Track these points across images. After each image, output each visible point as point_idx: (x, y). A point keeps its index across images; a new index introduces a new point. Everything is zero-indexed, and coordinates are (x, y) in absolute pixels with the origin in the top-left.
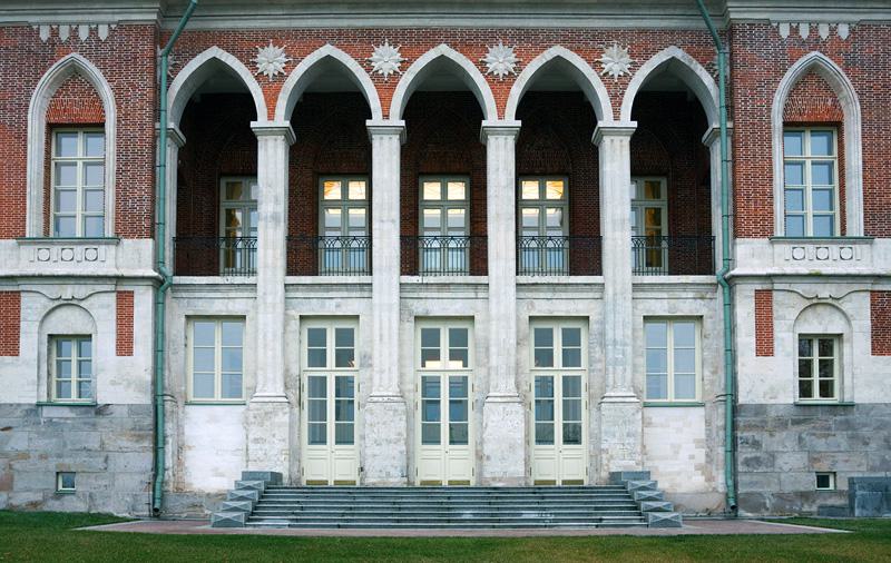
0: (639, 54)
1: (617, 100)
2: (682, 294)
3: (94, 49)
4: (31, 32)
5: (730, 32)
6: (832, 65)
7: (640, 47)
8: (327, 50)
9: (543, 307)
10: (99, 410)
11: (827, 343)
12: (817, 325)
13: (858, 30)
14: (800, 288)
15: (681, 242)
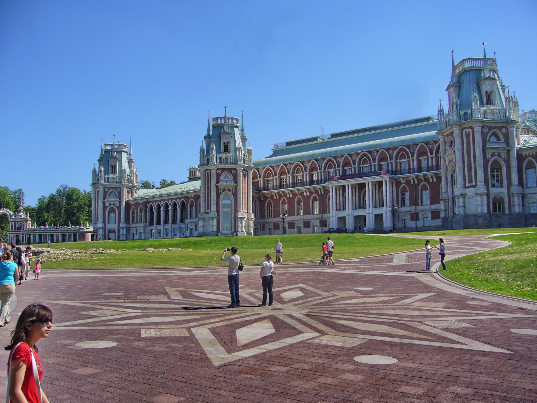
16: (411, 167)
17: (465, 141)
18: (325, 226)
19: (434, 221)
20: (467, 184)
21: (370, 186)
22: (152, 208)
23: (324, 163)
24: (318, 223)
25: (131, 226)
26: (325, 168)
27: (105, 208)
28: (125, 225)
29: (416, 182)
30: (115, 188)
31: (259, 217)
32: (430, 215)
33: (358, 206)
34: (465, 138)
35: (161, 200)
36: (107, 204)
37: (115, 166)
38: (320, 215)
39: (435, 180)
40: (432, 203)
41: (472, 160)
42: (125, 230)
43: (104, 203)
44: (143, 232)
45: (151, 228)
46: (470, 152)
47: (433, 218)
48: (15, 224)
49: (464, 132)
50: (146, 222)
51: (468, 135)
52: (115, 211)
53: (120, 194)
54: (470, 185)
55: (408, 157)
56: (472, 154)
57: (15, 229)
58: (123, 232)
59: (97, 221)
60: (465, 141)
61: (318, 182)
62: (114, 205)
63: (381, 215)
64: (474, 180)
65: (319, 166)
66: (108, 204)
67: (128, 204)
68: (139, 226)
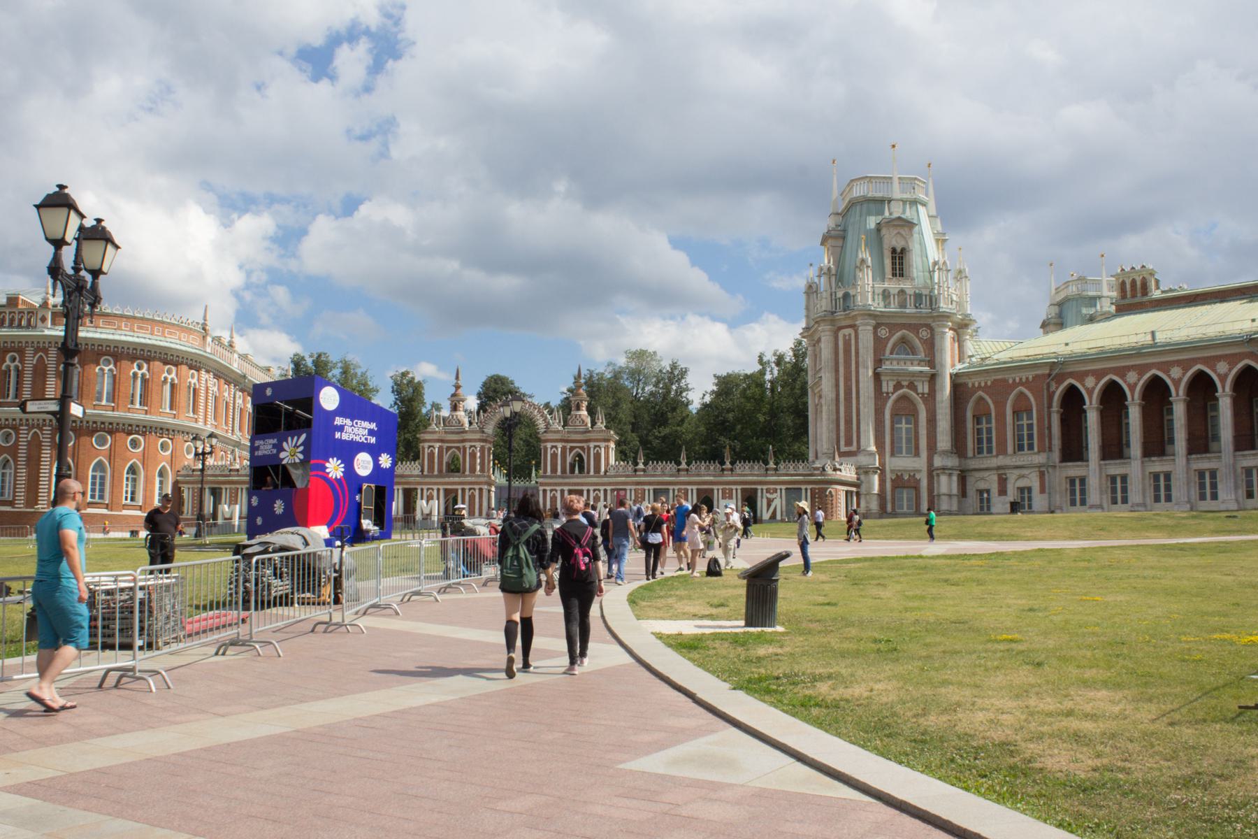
22: (1073, 399)
25: (973, 464)
27: (880, 397)
28: (952, 462)
30: (915, 328)
35: (1129, 368)
36: (888, 386)
37: (903, 250)
42: (955, 478)
43: (877, 377)
44: (1036, 485)
45: (1074, 470)
48: (564, 449)
50: (1050, 449)
52: (914, 414)
53: (931, 346)
57: (564, 471)
58: (947, 485)
59: (849, 443)
62: (912, 386)
66: (891, 384)
67: (959, 387)
68: (1025, 466)
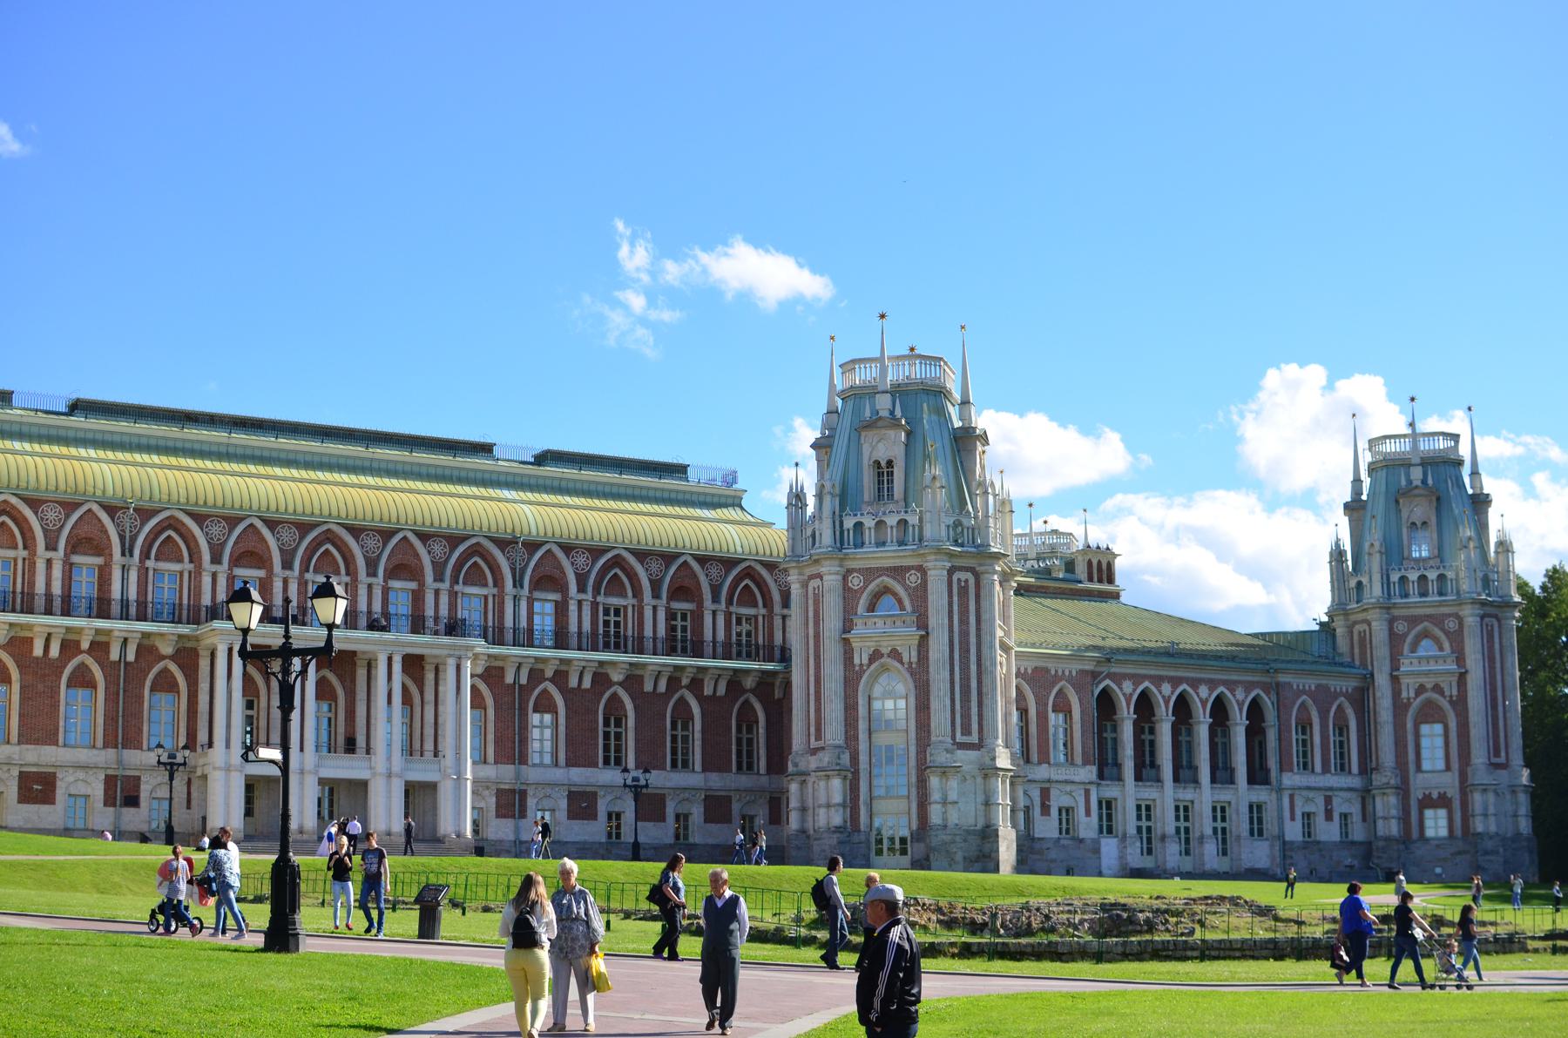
0: (1247, 691)
1: (1241, 710)
2: (1261, 794)
3: (1070, 680)
4: (1047, 670)
5: (1278, 684)
6: (1310, 702)
7: (1249, 687)
8: (1146, 684)
9: (1216, 798)
10: (1081, 841)
11: (1309, 815)
12: (1307, 809)
13: (1318, 686)
14: (1305, 793)
15: (1258, 775)
16: (509, 622)
17: (956, 608)
18: (132, 801)
19: (577, 825)
20: (959, 738)
21: (397, 667)
23: (147, 529)
24: (98, 790)
26: (145, 555)
29: (524, 681)
31: (100, 743)
32: (564, 804)
33: (341, 740)
34: (955, 598)
38: (111, 753)
39: (587, 684)
40: (569, 764)
41: (973, 668)
46: (968, 644)
47: (572, 815)
49: (955, 578)
51: (963, 591)
54: (966, 739)
55: (498, 581)
56: (973, 650)
60: (956, 608)
61: (101, 608)
63: (432, 787)
64: (975, 727)
65: (122, 538)
